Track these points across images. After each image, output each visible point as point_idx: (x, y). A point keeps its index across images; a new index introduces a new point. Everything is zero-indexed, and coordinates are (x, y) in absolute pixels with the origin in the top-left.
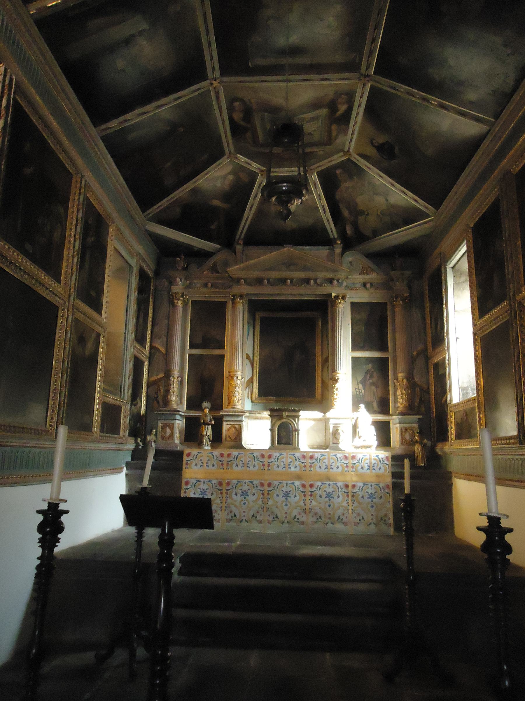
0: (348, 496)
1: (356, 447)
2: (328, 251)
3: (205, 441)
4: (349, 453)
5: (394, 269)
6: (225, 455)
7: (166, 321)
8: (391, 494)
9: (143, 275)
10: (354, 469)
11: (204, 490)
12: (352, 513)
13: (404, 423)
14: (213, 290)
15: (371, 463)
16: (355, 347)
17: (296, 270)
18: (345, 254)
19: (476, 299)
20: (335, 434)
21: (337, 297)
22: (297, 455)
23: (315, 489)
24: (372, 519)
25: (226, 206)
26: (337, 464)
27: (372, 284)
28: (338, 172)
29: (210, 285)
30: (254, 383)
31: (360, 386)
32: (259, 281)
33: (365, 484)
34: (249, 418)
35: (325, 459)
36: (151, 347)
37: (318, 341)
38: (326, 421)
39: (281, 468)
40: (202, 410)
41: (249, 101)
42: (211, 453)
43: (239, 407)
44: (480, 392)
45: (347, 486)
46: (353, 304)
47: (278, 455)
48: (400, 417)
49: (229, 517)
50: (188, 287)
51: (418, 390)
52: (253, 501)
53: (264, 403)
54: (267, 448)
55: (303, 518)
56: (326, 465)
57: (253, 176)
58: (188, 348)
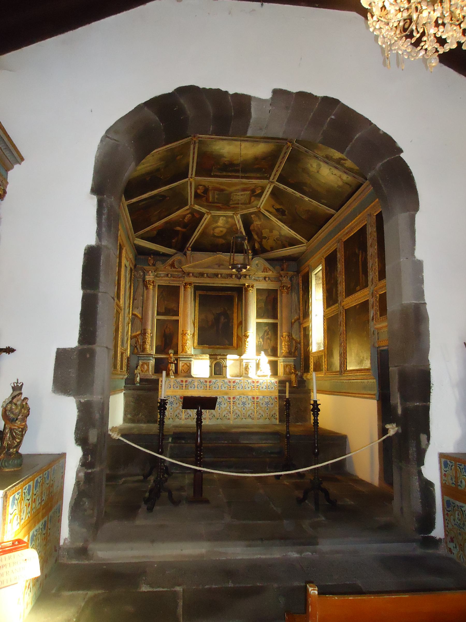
1: (259, 376)
3: (171, 372)
4: (255, 380)
7: (142, 298)
16: (258, 316)
19: (325, 297)
21: (248, 286)
22: (226, 380)
25: (184, 230)
28: (252, 216)
29: (170, 275)
31: (261, 340)
32: (202, 275)
36: (133, 314)
38: (241, 361)
39: (216, 388)
43: (189, 352)
45: (254, 398)
49: (187, 417)
51: (294, 342)
54: (208, 377)
57: (202, 215)
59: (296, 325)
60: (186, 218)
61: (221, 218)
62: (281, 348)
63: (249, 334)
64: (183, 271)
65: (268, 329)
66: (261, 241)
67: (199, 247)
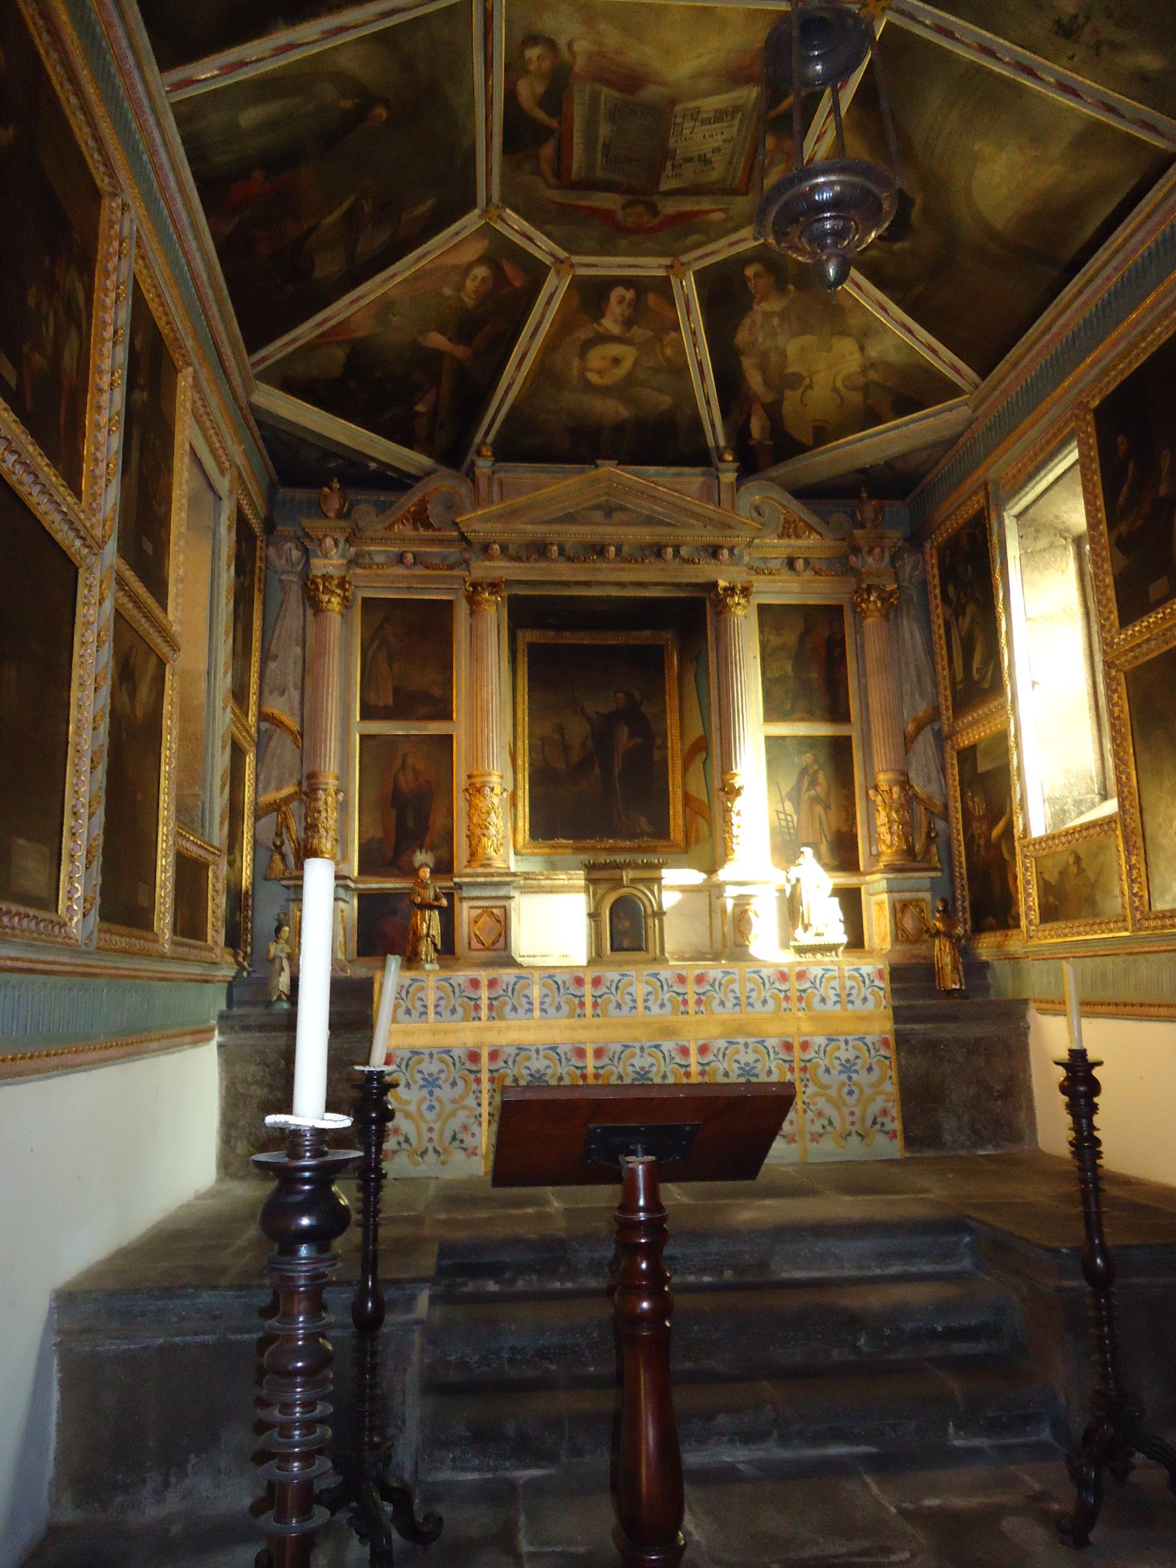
0: (792, 1069)
1: (801, 950)
2: (702, 479)
3: (425, 948)
5: (862, 526)
7: (298, 650)
8: (894, 1057)
9: (241, 521)
10: (803, 1005)
11: (431, 1075)
12: (805, 1111)
13: (898, 891)
14: (420, 571)
15: (843, 987)
16: (772, 712)
17: (628, 524)
18: (742, 489)
20: (740, 921)
21: (730, 590)
22: (665, 974)
23: (712, 1058)
24: (853, 1123)
25: (460, 351)
26: (764, 994)
27: (807, 562)
28: (750, 271)
29: (409, 558)
30: (520, 807)
32: (540, 550)
33: (830, 1040)
34: (525, 890)
35: (732, 981)
36: (262, 717)
37: (672, 702)
38: (713, 891)
39: (625, 1009)
40: (413, 872)
41: (570, 45)
42: (444, 980)
43: (498, 864)
44: (1127, 803)
45: (788, 1047)
46: (762, 609)
47: (617, 977)
48: (890, 876)
50: (353, 562)
51: (920, 811)
53: (543, 855)
56: (736, 998)
57: (536, 273)
58: (358, 718)
59: (925, 743)
60: (470, 285)
61: (618, 292)
62: (872, 838)
63: (737, 782)
64: (463, 537)
65: (815, 761)
66: (778, 403)
67: (526, 443)
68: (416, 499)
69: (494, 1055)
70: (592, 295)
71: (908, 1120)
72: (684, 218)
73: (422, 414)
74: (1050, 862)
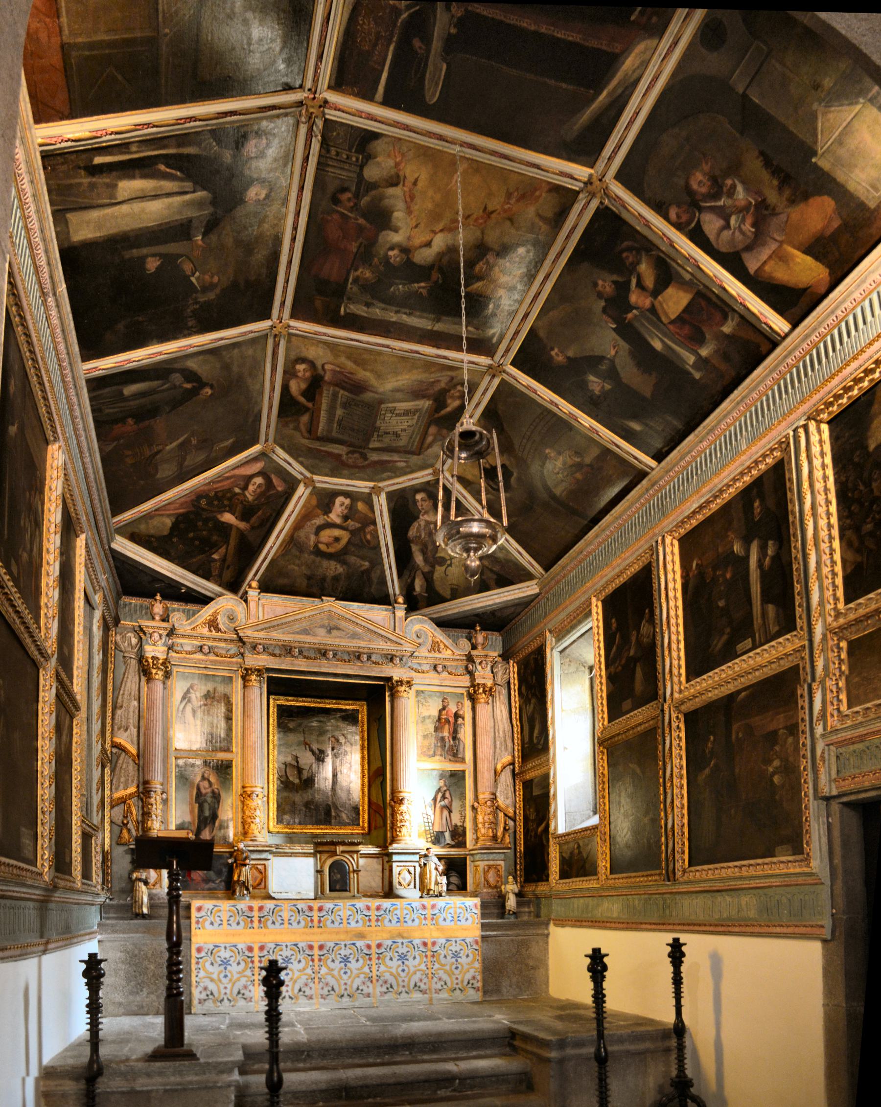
6: (256, 908)
39: (336, 924)
45: (425, 944)
52: (300, 971)
55: (369, 989)
68: (210, 612)
69: (262, 948)
70: (325, 500)
71: (485, 981)
72: (382, 463)
73: (215, 560)
74: (565, 847)
